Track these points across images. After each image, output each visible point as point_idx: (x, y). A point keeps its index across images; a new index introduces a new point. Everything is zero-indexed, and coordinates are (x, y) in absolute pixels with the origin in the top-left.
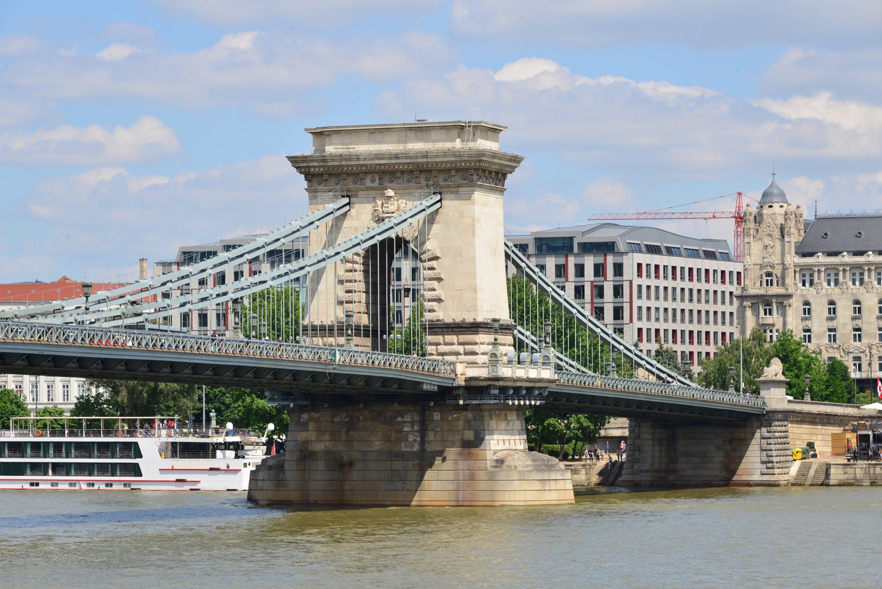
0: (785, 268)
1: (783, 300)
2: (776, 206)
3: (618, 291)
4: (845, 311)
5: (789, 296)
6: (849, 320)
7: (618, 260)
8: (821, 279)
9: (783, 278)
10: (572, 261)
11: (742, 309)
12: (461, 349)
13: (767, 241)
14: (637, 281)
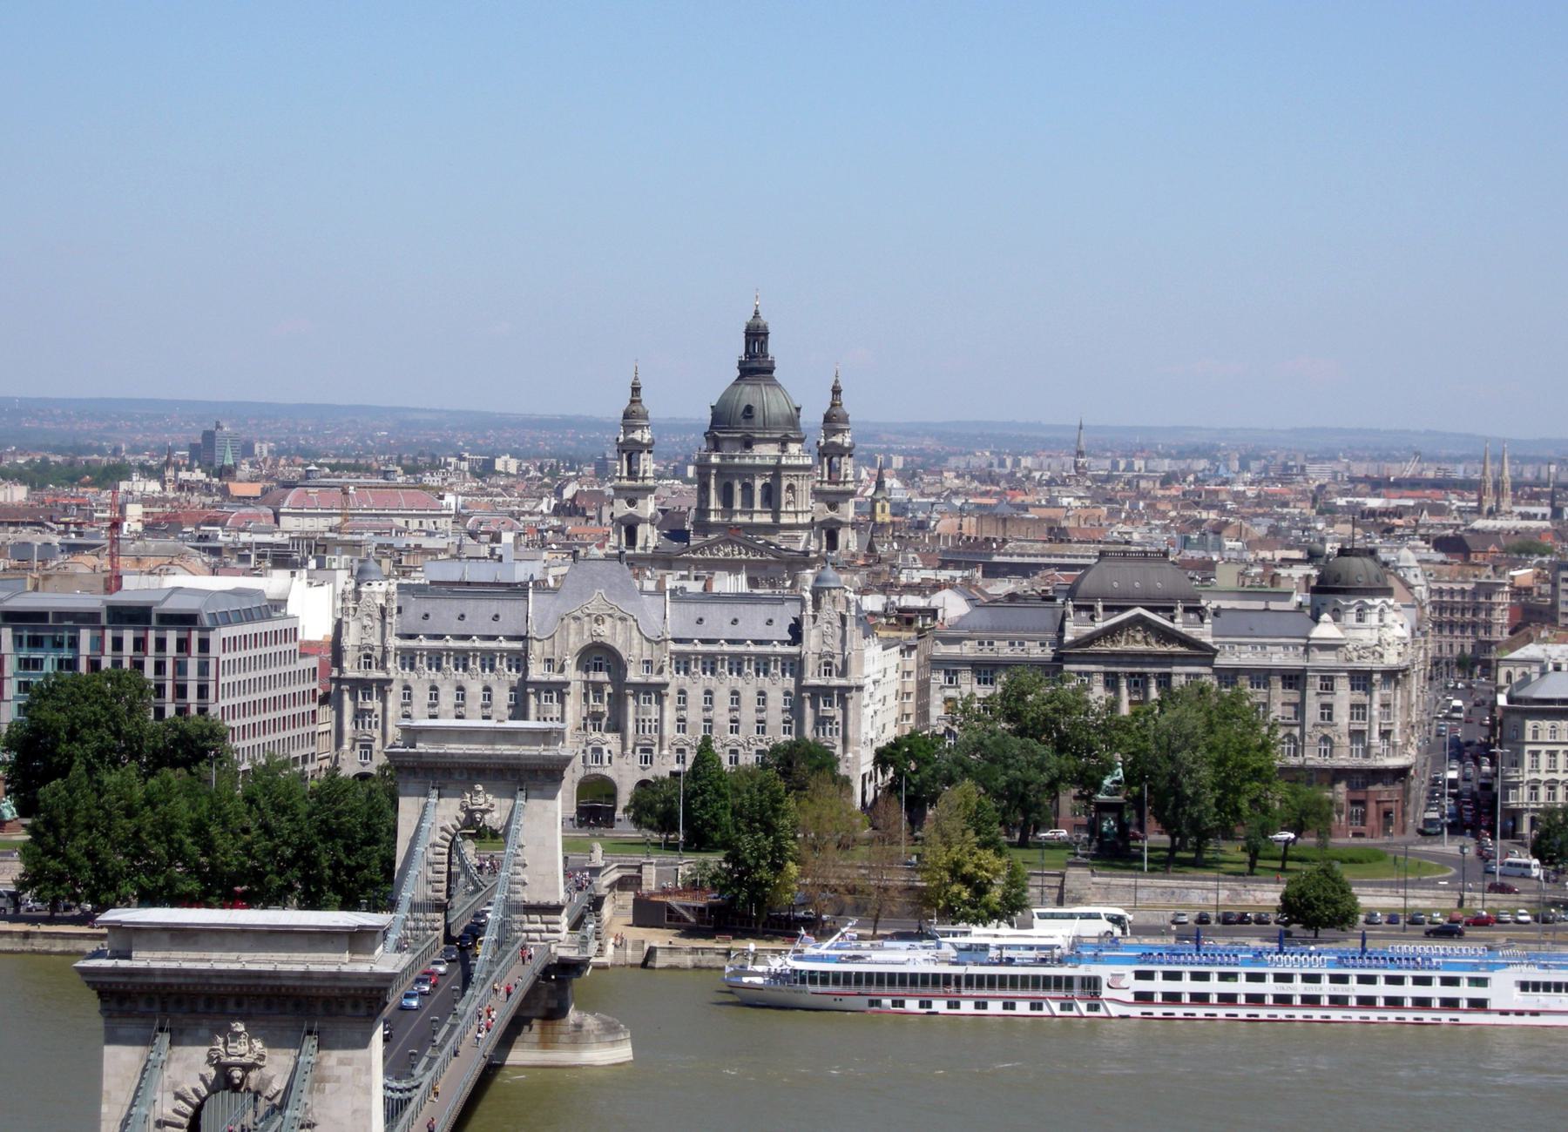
0: (385, 652)
1: (383, 686)
2: (375, 584)
3: (203, 669)
4: (447, 698)
5: (390, 681)
6: (451, 707)
7: (204, 635)
8: (421, 664)
9: (384, 660)
10: (152, 636)
11: (340, 693)
12: (544, 927)
13: (366, 621)
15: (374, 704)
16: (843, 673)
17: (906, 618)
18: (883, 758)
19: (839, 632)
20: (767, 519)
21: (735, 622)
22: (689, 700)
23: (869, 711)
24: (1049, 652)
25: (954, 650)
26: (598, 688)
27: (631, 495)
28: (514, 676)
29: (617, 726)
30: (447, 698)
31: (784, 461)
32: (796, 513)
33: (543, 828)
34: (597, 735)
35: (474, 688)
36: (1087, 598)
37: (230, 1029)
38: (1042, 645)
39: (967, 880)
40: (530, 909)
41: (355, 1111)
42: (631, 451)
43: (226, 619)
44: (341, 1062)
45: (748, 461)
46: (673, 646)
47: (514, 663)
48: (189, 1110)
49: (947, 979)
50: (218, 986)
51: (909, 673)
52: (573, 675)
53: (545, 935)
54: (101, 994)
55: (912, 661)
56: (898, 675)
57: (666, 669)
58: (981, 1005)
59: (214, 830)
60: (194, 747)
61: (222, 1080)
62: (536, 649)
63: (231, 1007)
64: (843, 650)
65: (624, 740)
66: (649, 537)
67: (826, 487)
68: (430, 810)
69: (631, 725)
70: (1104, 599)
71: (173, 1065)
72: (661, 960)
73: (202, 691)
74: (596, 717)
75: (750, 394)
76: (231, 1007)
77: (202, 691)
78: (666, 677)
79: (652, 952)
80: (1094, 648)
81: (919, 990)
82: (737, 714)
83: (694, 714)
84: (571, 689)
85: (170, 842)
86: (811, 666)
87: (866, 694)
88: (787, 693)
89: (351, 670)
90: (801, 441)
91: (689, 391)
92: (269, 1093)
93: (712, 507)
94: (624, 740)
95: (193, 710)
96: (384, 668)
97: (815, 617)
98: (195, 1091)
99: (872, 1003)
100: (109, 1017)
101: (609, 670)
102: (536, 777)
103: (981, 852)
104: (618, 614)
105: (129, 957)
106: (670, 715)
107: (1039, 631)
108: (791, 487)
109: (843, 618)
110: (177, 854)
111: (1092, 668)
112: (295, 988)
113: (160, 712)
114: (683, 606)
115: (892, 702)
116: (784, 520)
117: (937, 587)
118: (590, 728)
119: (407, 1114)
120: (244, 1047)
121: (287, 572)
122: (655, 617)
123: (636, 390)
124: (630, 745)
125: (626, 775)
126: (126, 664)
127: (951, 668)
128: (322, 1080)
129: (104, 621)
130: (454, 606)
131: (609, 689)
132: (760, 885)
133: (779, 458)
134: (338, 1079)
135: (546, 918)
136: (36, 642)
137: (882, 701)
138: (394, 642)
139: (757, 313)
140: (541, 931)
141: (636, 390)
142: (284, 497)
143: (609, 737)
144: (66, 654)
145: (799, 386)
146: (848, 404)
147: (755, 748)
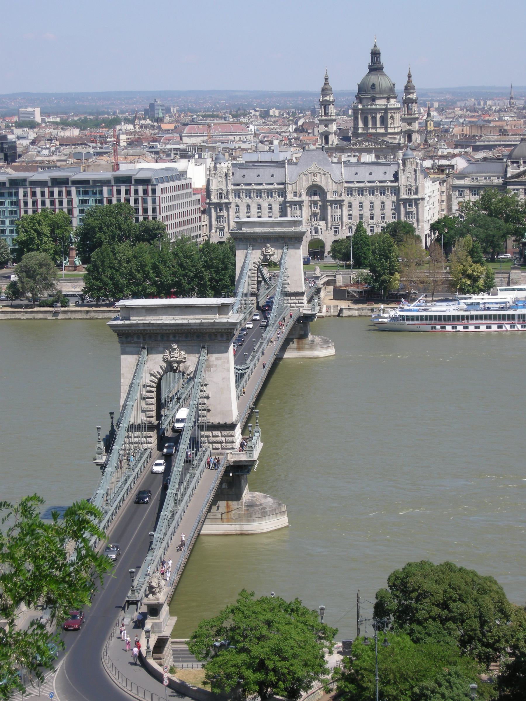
0: (228, 191)
1: (227, 205)
2: (222, 163)
3: (154, 201)
4: (254, 209)
5: (230, 203)
6: (256, 213)
7: (154, 187)
8: (243, 196)
9: (227, 195)
10: (132, 188)
11: (210, 209)
12: (297, 301)
13: (219, 179)
14: (162, 196)
15: (224, 213)
16: (416, 193)
17: (441, 169)
18: (434, 227)
19: (414, 176)
20: (382, 131)
21: (371, 173)
22: (353, 207)
23: (427, 209)
24: (501, 181)
25: (462, 182)
26: (315, 203)
27: (326, 123)
28: (281, 199)
29: (324, 218)
30: (254, 209)
31: (389, 106)
32: (395, 128)
33: (294, 259)
34: (316, 222)
35: (265, 205)
36: (516, 158)
37: (171, 347)
38: (498, 178)
39: (469, 277)
40: (291, 294)
41: (223, 379)
42: (325, 104)
43: (163, 180)
44: (217, 359)
45: (374, 107)
46: (346, 185)
47: (280, 194)
48: (156, 380)
49: (463, 317)
50: (166, 330)
51: (443, 192)
52: (305, 198)
53: (298, 305)
54: (118, 335)
55: (444, 187)
56: (439, 193)
57: (343, 194)
58: (477, 327)
59: (161, 267)
60: (152, 233)
61: (169, 368)
62: (289, 188)
63: (171, 338)
64: (416, 183)
65: (327, 224)
66: (334, 140)
67: (407, 116)
68: (249, 255)
69: (329, 218)
70: (523, 158)
71: (149, 362)
72: (345, 313)
73: (154, 210)
74: (315, 215)
75: (374, 79)
76: (171, 338)
77: (154, 210)
78: (343, 197)
79: (341, 310)
80: (520, 179)
81: (451, 322)
82: (373, 211)
83: (355, 212)
84: (304, 204)
85: (144, 272)
86: (403, 190)
87: (426, 201)
88: (393, 202)
89: (214, 199)
90: (395, 98)
91: (348, 79)
92: (188, 372)
93: (360, 126)
94: (327, 224)
95: (151, 218)
96: (227, 198)
97: (404, 170)
98: (158, 372)
99: (432, 328)
100: (123, 344)
101: (319, 195)
102: (292, 240)
103: (474, 265)
104: (322, 172)
105: (129, 320)
106: (345, 213)
107: (497, 172)
108: (392, 117)
109: (415, 170)
110: (146, 277)
111: (519, 187)
112: (197, 329)
113: (137, 220)
114: (349, 168)
115: (436, 204)
116: (390, 131)
117: (454, 156)
118: (313, 220)
119: (244, 379)
120: (178, 354)
121: (187, 160)
122: (338, 173)
123: (326, 79)
124: (329, 226)
125: (328, 238)
126: (123, 201)
127: (460, 189)
128: (209, 366)
129: (113, 183)
130: (256, 171)
131: (320, 203)
132: (384, 281)
133: (387, 105)
134: (216, 366)
135: (298, 298)
136: (86, 193)
137: (433, 203)
138: (231, 187)
139: (375, 45)
140: (296, 303)
141: (326, 79)
142: (184, 129)
143: (320, 223)
144: (98, 197)
145: (394, 75)
146: (415, 82)
147: (381, 225)
